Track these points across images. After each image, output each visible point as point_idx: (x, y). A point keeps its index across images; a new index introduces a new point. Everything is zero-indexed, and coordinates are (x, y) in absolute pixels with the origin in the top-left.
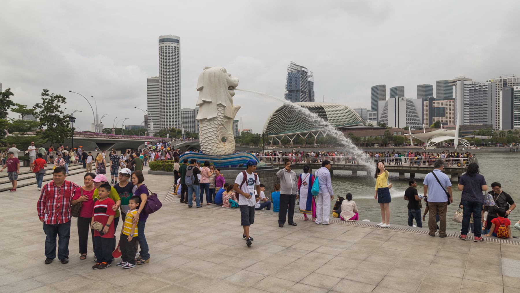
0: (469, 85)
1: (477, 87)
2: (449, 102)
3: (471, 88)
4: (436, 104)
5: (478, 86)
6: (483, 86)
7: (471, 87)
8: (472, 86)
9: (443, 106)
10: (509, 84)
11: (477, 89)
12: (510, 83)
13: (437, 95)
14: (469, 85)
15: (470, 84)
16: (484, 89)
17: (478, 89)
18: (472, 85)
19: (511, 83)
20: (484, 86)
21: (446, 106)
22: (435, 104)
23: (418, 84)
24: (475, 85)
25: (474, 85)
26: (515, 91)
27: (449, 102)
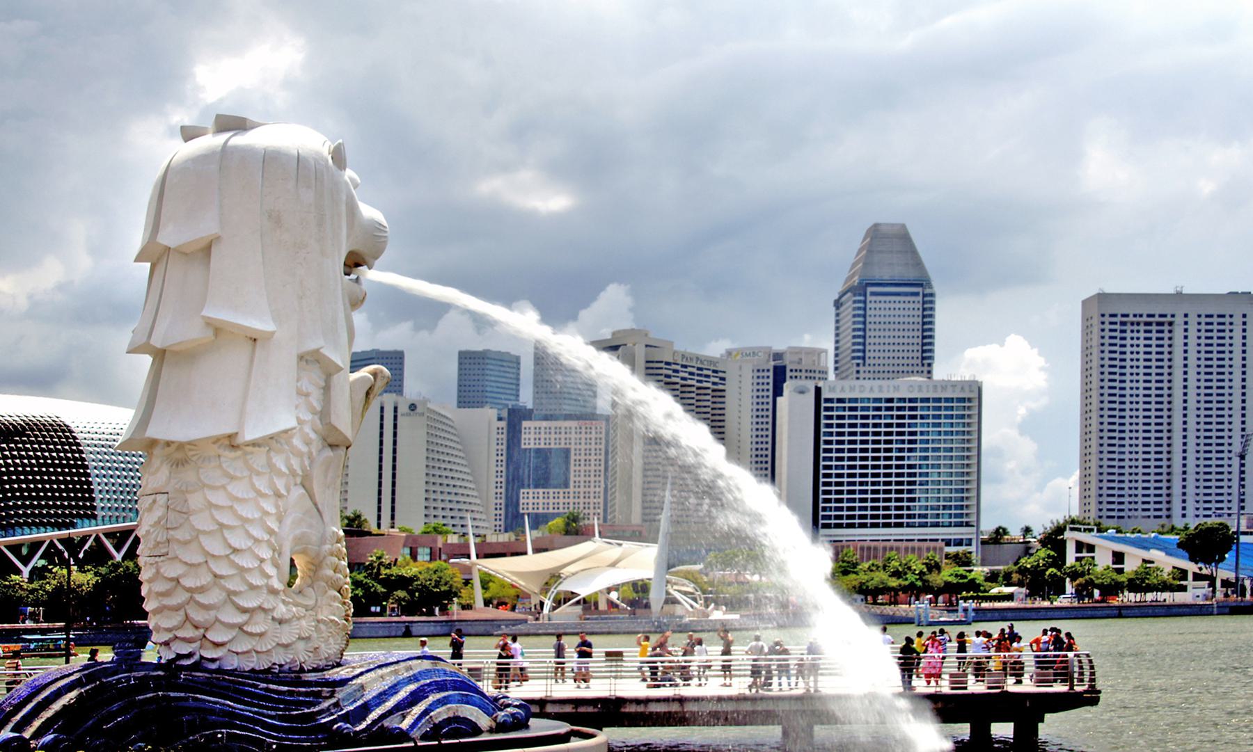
0: (662, 365)
1: (691, 374)
2: (583, 430)
3: (669, 376)
4: (533, 435)
5: (694, 370)
6: (709, 373)
7: (670, 372)
8: (676, 371)
9: (563, 446)
10: (791, 371)
11: (689, 382)
12: (794, 368)
13: (535, 398)
14: (662, 365)
15: (668, 363)
16: (714, 383)
17: (693, 382)
18: (674, 367)
19: (798, 367)
20: (714, 371)
21: (573, 447)
22: (532, 436)
23: (463, 349)
24: (685, 366)
25: (683, 366)
26: (827, 400)
27: (583, 430)
